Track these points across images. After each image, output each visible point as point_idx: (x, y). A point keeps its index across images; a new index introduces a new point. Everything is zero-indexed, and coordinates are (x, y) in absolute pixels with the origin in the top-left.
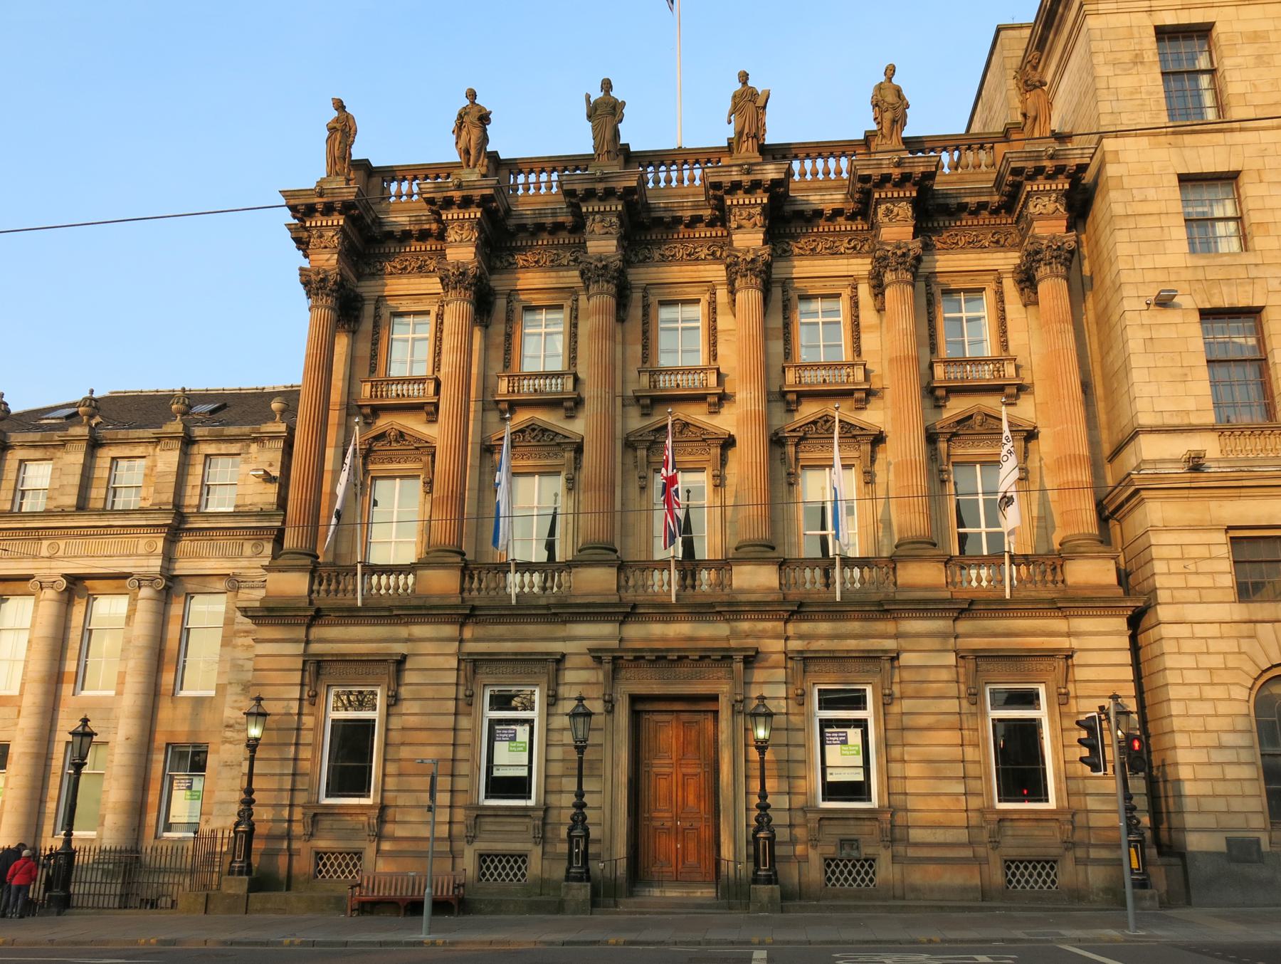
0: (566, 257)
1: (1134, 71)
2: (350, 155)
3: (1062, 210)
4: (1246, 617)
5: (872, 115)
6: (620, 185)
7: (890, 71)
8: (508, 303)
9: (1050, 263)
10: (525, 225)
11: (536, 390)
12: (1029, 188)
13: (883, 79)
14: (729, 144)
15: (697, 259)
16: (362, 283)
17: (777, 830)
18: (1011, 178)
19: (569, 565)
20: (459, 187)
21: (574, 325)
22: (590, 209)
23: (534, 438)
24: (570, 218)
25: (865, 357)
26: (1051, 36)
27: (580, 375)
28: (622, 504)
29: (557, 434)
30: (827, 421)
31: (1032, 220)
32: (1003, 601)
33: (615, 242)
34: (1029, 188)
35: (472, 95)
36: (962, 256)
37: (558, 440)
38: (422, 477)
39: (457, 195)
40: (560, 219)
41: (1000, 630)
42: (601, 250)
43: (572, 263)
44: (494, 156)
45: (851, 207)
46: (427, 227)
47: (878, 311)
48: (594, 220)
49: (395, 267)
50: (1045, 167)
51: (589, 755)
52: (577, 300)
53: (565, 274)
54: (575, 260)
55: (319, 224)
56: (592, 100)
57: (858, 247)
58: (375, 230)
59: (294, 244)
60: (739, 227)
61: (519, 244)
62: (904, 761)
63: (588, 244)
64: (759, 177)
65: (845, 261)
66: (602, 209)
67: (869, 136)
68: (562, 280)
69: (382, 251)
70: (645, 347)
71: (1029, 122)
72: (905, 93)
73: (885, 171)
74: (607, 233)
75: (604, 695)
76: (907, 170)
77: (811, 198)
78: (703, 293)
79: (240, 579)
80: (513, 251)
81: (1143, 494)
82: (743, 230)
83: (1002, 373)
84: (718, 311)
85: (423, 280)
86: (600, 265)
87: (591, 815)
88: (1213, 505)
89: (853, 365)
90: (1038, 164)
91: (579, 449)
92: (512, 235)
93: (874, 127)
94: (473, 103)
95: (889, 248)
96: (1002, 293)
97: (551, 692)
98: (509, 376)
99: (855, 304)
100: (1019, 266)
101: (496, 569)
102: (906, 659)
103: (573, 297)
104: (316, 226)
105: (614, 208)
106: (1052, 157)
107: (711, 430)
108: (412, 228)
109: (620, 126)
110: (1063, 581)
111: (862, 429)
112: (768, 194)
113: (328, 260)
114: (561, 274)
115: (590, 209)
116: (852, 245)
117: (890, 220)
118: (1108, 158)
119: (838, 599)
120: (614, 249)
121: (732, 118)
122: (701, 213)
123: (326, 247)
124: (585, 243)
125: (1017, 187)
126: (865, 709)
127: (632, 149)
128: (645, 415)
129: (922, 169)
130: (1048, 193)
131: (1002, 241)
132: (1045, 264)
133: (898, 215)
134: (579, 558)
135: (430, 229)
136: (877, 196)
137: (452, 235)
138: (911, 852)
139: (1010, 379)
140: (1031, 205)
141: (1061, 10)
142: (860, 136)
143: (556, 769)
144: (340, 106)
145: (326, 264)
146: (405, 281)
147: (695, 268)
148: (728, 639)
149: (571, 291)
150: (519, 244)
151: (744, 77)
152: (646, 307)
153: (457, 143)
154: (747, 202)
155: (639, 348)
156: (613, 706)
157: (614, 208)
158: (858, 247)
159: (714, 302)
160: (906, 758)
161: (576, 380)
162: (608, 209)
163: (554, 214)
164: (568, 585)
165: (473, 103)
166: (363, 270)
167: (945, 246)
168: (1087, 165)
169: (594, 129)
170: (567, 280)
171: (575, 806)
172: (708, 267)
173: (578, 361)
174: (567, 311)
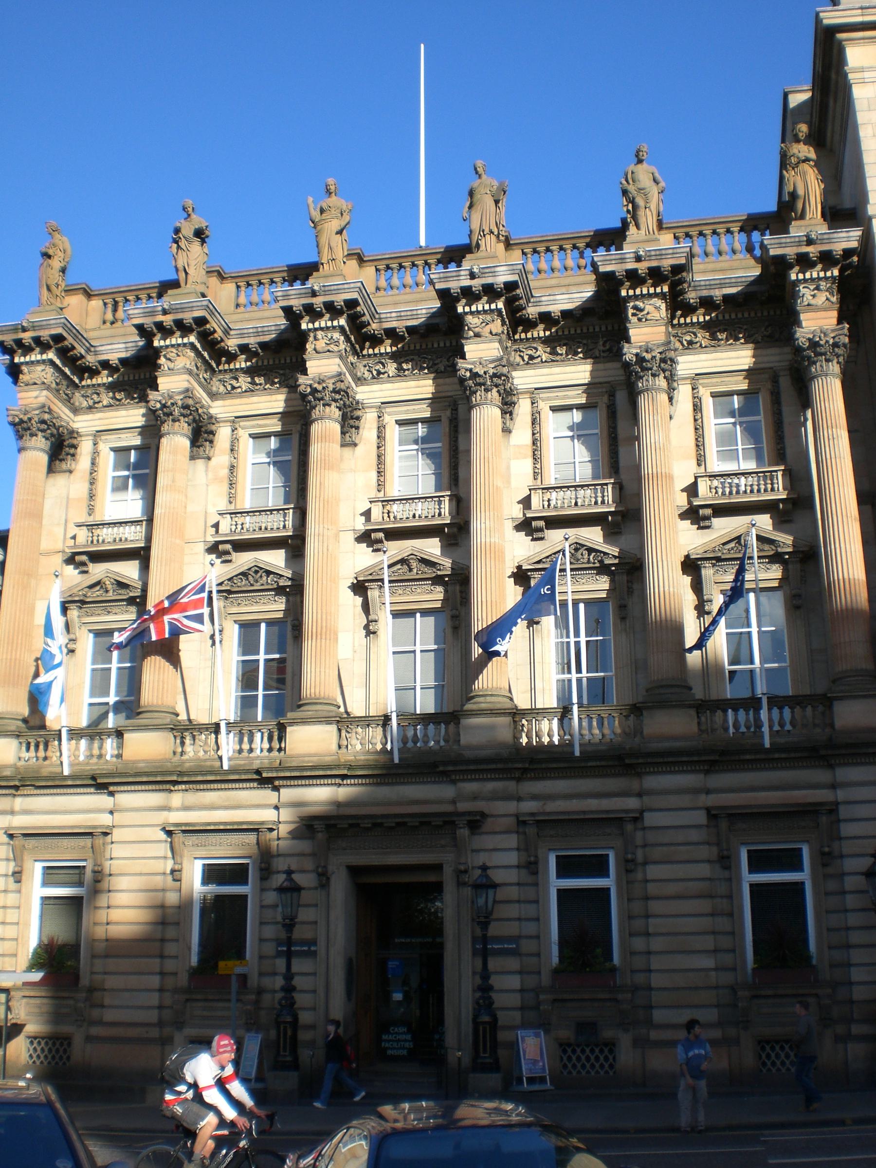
17: (500, 1014)
32: (759, 748)
51: (299, 933)
62: (648, 934)
64: (489, 280)
73: (631, 266)
75: (318, 867)
76: (654, 264)
87: (301, 999)
97: (263, 865)
102: (650, 819)
110: (832, 725)
113: (36, 397)
116: (608, 347)
117: (640, 320)
119: (577, 753)
123: (35, 384)
126: (608, 876)
138: (654, 1035)
143: (269, 949)
145: (35, 401)
148: (454, 802)
156: (328, 879)
159: (456, 419)
160: (651, 930)
171: (283, 989)
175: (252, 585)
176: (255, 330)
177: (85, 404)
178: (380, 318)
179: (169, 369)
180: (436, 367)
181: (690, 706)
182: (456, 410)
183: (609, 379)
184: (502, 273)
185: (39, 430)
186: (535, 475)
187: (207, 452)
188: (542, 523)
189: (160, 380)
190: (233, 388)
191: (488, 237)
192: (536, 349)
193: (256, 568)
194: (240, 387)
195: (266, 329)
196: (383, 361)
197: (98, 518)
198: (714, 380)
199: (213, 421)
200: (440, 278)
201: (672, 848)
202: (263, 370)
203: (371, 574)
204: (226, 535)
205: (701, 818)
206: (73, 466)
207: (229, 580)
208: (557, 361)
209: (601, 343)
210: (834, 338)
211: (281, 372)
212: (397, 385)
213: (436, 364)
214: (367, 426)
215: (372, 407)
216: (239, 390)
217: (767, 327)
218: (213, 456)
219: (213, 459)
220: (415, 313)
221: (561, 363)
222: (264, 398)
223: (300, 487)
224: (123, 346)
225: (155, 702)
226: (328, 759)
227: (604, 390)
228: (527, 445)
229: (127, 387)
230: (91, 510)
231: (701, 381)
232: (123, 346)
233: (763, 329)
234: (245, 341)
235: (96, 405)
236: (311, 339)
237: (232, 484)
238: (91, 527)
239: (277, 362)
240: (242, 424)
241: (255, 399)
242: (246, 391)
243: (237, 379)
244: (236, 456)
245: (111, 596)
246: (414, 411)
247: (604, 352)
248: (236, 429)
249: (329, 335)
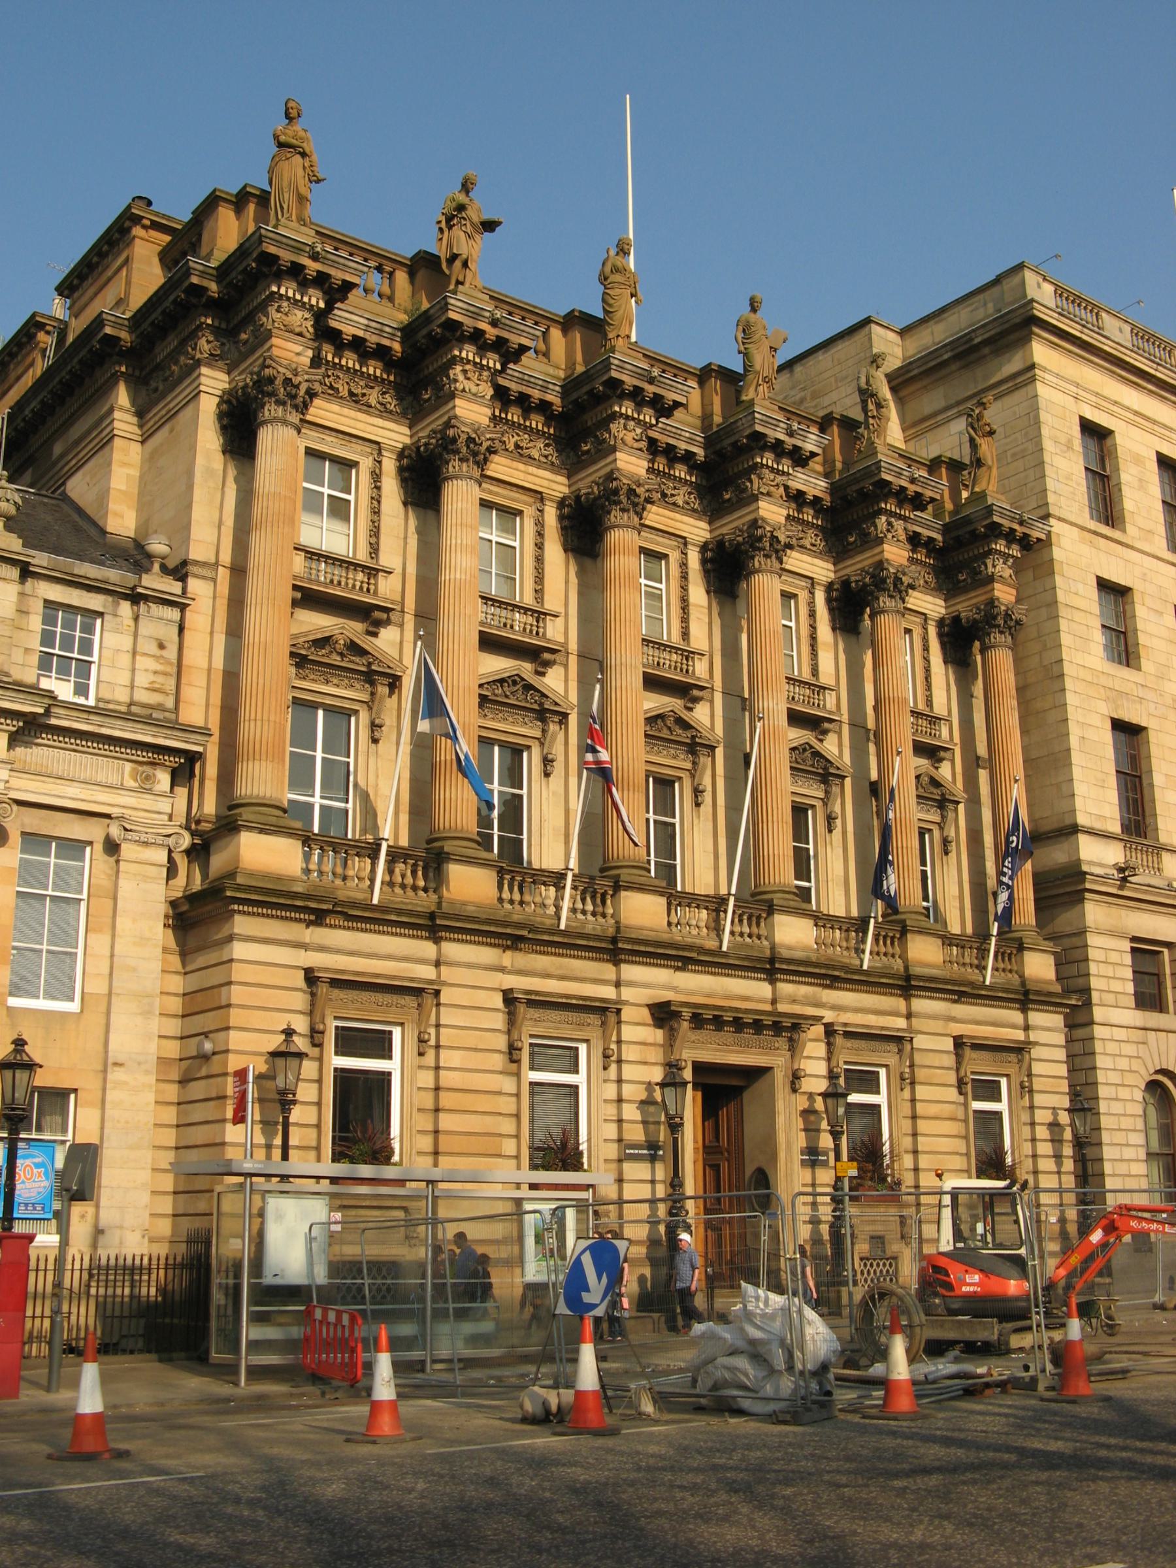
1: (1066, 455)
4: (1139, 1024)
26: (954, 367)
30: (805, 750)
40: (549, 398)
41: (979, 1018)
60: (769, 494)
64: (799, 443)
65: (809, 559)
68: (531, 478)
79: (128, 827)
81: (1087, 895)
88: (1123, 913)
102: (920, 1042)
113: (298, 354)
163: (544, 389)
170: (538, 481)
176: (521, 376)
195: (532, 380)
201: (932, 1070)
205: (949, 1044)
226: (651, 935)
245: (335, 659)
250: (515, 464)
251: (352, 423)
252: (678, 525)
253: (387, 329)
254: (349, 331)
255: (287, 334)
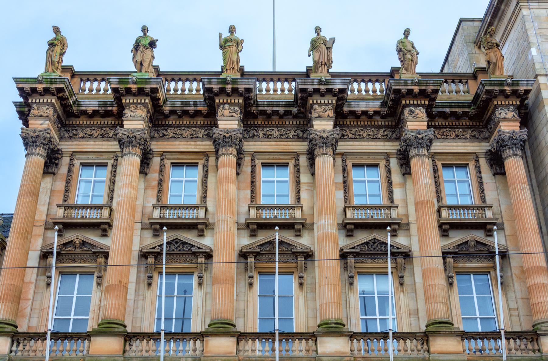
0: (202, 133)
2: (62, 61)
3: (516, 116)
5: (397, 57)
6: (241, 87)
7: (407, 33)
8: (161, 160)
9: (512, 148)
10: (176, 110)
11: (179, 217)
12: (495, 103)
13: (403, 37)
14: (308, 70)
15: (287, 138)
16: (63, 143)
18: (484, 96)
19: (202, 336)
20: (135, 83)
21: (205, 176)
22: (221, 101)
23: (177, 248)
24: (206, 108)
25: (396, 202)
26: (496, 23)
27: (209, 208)
28: (237, 296)
29: (193, 246)
30: (374, 243)
31: (499, 122)
33: (237, 122)
34: (495, 103)
35: (145, 30)
36: (454, 144)
37: (194, 249)
38: (96, 274)
39: (134, 87)
40: (199, 108)
42: (228, 127)
43: (205, 137)
44: (156, 69)
45: (385, 110)
46: (110, 108)
47: (404, 175)
48: (223, 108)
49: (85, 134)
50: (505, 90)
52: (207, 160)
53: (200, 143)
54: (208, 135)
55: (38, 101)
56: (223, 37)
57: (389, 136)
58: (75, 108)
59: (17, 115)
60: (319, 117)
61: (171, 123)
63: (219, 122)
64: (331, 87)
65: (382, 144)
66: (229, 101)
67: (394, 71)
68: (198, 147)
69: (78, 123)
70: (252, 192)
71: (491, 66)
72: (415, 45)
74: (232, 116)
76: (423, 88)
77: (361, 103)
78: (291, 159)
80: (166, 127)
82: (320, 119)
83: (484, 215)
84: (302, 170)
85: (104, 143)
86: (227, 135)
89: (390, 207)
90: (502, 88)
91: (209, 256)
92: (167, 117)
93: (398, 64)
94: (145, 34)
95: (413, 134)
96: (479, 167)
98: (161, 207)
99: (389, 171)
100: (490, 151)
101: (149, 337)
103: (205, 158)
104: (36, 103)
105: (237, 101)
106: (508, 85)
107: (298, 246)
108: (100, 109)
109: (240, 54)
111: (398, 248)
112: (336, 98)
113: (41, 124)
114: (198, 143)
115: (221, 101)
116: (386, 133)
118: (542, 87)
120: (236, 127)
121: (311, 53)
122: (291, 109)
123: (41, 116)
124: (217, 123)
125: (487, 102)
127: (246, 70)
128: (253, 234)
129: (432, 87)
130: (507, 106)
131: (477, 136)
132: (509, 148)
133: (417, 114)
134: (211, 330)
135: (111, 111)
136: (404, 102)
137: (127, 113)
139: (489, 219)
140: (497, 113)
141: (503, 7)
142: (388, 71)
144: (57, 30)
145: (41, 126)
146: (92, 143)
147: (286, 143)
149: (205, 155)
150: (171, 123)
151: (318, 30)
152: (253, 167)
153: (134, 58)
154: (323, 102)
155: (249, 192)
157: (237, 101)
158: (389, 136)
161: (206, 211)
162: (233, 101)
163: (195, 105)
164: (201, 349)
165: (145, 34)
166: (64, 135)
167: (443, 137)
168: (530, 90)
169: (224, 54)
170: (202, 147)
172: (294, 143)
173: (208, 199)
174: (200, 167)
175: (173, 250)
177: (67, 135)
178: (257, 104)
179: (131, 116)
180: (287, 135)
181: (457, 336)
182: (298, 160)
183: (386, 151)
184: (338, 84)
185: (42, 143)
186: (346, 200)
187: (145, 170)
188: (352, 227)
189: (125, 123)
190: (164, 135)
191: (323, 66)
192: (346, 132)
193: (177, 240)
194: (168, 135)
196: (256, 129)
197: (70, 202)
198: (444, 157)
199: (151, 152)
200: (302, 82)
202: (183, 127)
203: (251, 249)
204: (157, 219)
206: (56, 172)
207: (159, 246)
208: (358, 138)
209: (382, 131)
210: (520, 136)
211: (194, 129)
212: (263, 143)
213: (287, 134)
214: (245, 164)
215: (248, 154)
216: (167, 137)
217: (472, 131)
218: (149, 173)
219: (148, 175)
220: (278, 103)
221: (360, 140)
222: (182, 143)
223: (203, 195)
224: (98, 103)
225: (112, 317)
227: (383, 157)
228: (340, 183)
229: (96, 129)
230: (66, 198)
231: (436, 157)
232: (98, 103)
233: (470, 132)
234: (175, 108)
235: (75, 137)
236: (221, 108)
237: (159, 191)
238: (67, 207)
239: (192, 123)
240: (167, 156)
241: (177, 143)
242: (171, 138)
243: (167, 130)
244: (163, 174)
245: (78, 250)
246: (273, 159)
247: (383, 136)
248: (164, 159)
249: (232, 108)
250: (189, 143)
251: (100, 147)
252: (290, 147)
253: (108, 103)
254: (90, 109)
255: (35, 118)
